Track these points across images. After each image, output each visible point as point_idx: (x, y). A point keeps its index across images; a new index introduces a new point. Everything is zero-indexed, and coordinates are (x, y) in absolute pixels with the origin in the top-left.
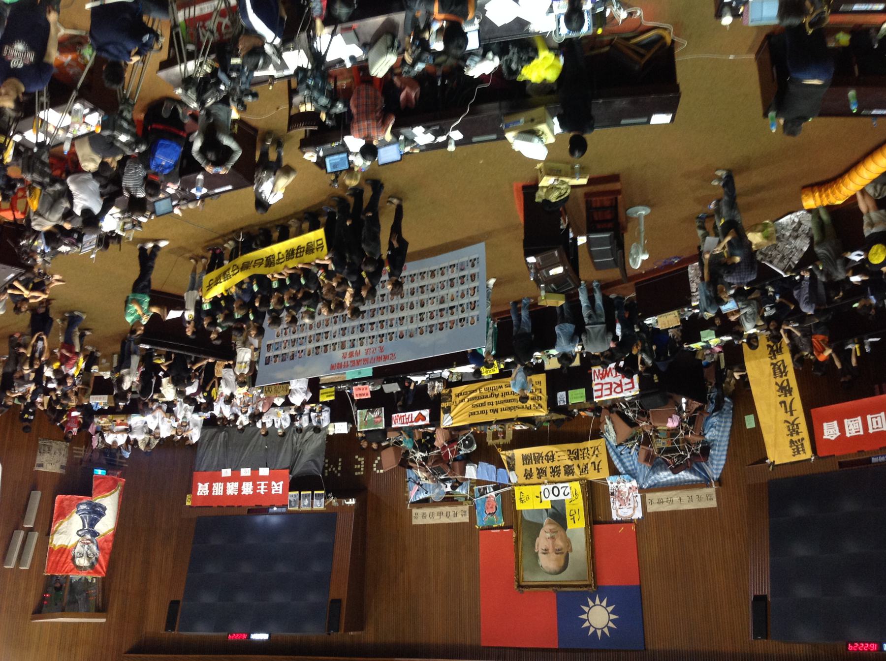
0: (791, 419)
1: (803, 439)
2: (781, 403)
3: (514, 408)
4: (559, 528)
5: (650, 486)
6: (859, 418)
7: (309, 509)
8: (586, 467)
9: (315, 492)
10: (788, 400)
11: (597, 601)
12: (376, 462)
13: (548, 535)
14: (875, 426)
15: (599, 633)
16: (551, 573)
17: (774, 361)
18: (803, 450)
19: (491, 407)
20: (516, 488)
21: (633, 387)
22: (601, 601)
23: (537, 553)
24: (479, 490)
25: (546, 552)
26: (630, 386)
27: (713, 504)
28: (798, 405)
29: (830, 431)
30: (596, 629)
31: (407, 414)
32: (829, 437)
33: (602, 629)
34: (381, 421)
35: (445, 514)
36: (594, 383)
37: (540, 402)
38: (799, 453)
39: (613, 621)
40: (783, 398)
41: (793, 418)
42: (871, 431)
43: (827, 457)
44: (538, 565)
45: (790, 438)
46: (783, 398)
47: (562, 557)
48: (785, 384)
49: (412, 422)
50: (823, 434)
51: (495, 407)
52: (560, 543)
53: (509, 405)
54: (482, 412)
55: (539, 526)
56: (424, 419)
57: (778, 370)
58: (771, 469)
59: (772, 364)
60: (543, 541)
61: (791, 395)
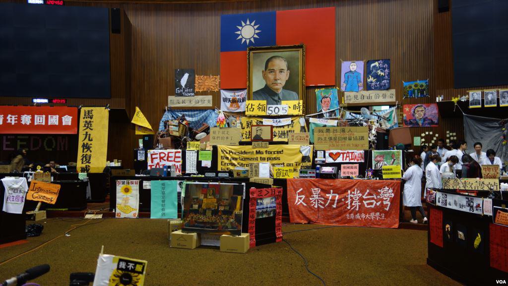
0: (88, 130)
1: (84, 118)
2: (92, 140)
3: (242, 153)
4: (272, 86)
5: (206, 110)
6: (49, 124)
7: (486, 91)
8: (248, 126)
9: (480, 106)
10: (86, 141)
11: (248, 41)
12: (433, 142)
13: (279, 82)
14: (41, 118)
15: (248, 23)
16: (279, 57)
17: (87, 164)
18: (85, 112)
19: (263, 156)
20: (301, 113)
21: (152, 155)
22: (245, 41)
23: (289, 68)
24: (335, 115)
25: (281, 71)
26: (154, 156)
27: (170, 98)
28: (81, 137)
29: (67, 120)
30: (250, 25)
31: (347, 161)
32: (69, 117)
33: (246, 25)
34: (376, 157)
35: (365, 98)
36: (181, 163)
37: (223, 155)
38: (89, 111)
39: (239, 30)
40: (90, 143)
41: (86, 131)
42: (44, 116)
43: (72, 106)
44: (287, 62)
45: (92, 120)
46: (90, 143)
47: (270, 67)
48: (85, 150)
49: (343, 154)
50: (72, 119)
51: (259, 156)
52: (271, 76)
53: (245, 156)
54: (271, 153)
55: (285, 88)
56: (331, 155)
57: (87, 158)
58: (108, 105)
59: (90, 163)
60: (283, 78)
61: (84, 143)
